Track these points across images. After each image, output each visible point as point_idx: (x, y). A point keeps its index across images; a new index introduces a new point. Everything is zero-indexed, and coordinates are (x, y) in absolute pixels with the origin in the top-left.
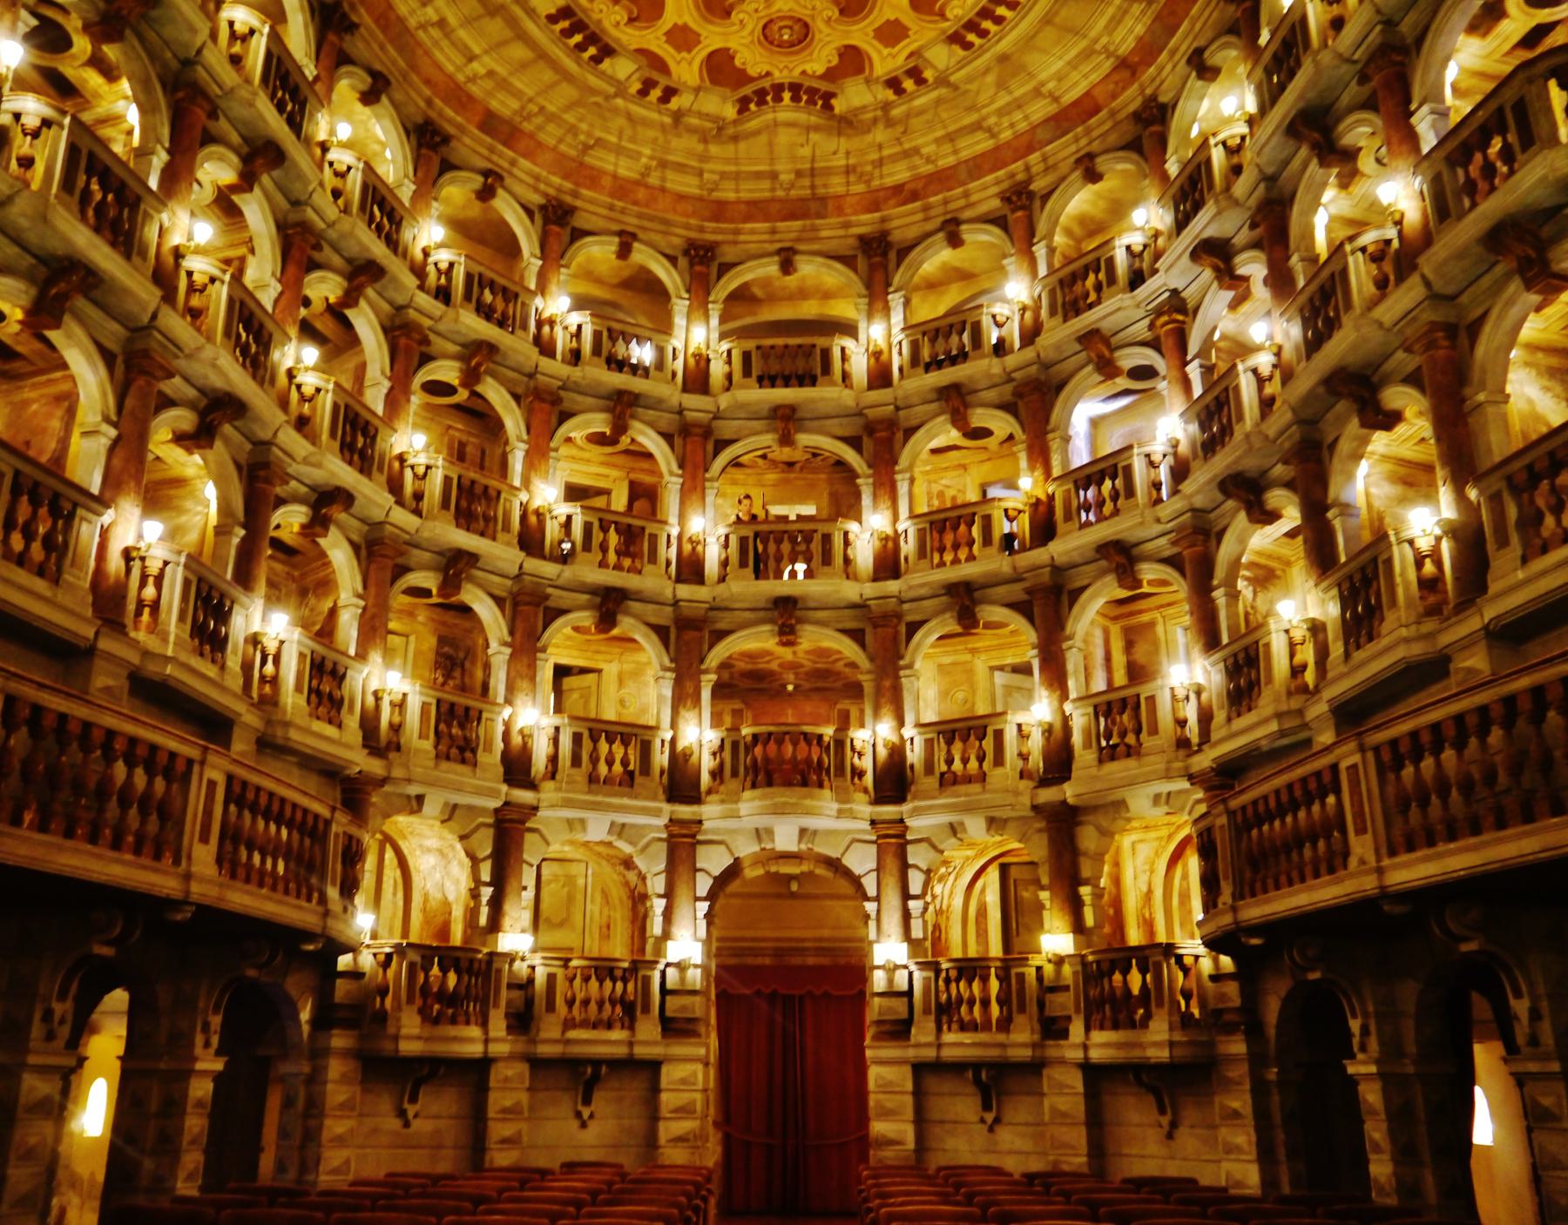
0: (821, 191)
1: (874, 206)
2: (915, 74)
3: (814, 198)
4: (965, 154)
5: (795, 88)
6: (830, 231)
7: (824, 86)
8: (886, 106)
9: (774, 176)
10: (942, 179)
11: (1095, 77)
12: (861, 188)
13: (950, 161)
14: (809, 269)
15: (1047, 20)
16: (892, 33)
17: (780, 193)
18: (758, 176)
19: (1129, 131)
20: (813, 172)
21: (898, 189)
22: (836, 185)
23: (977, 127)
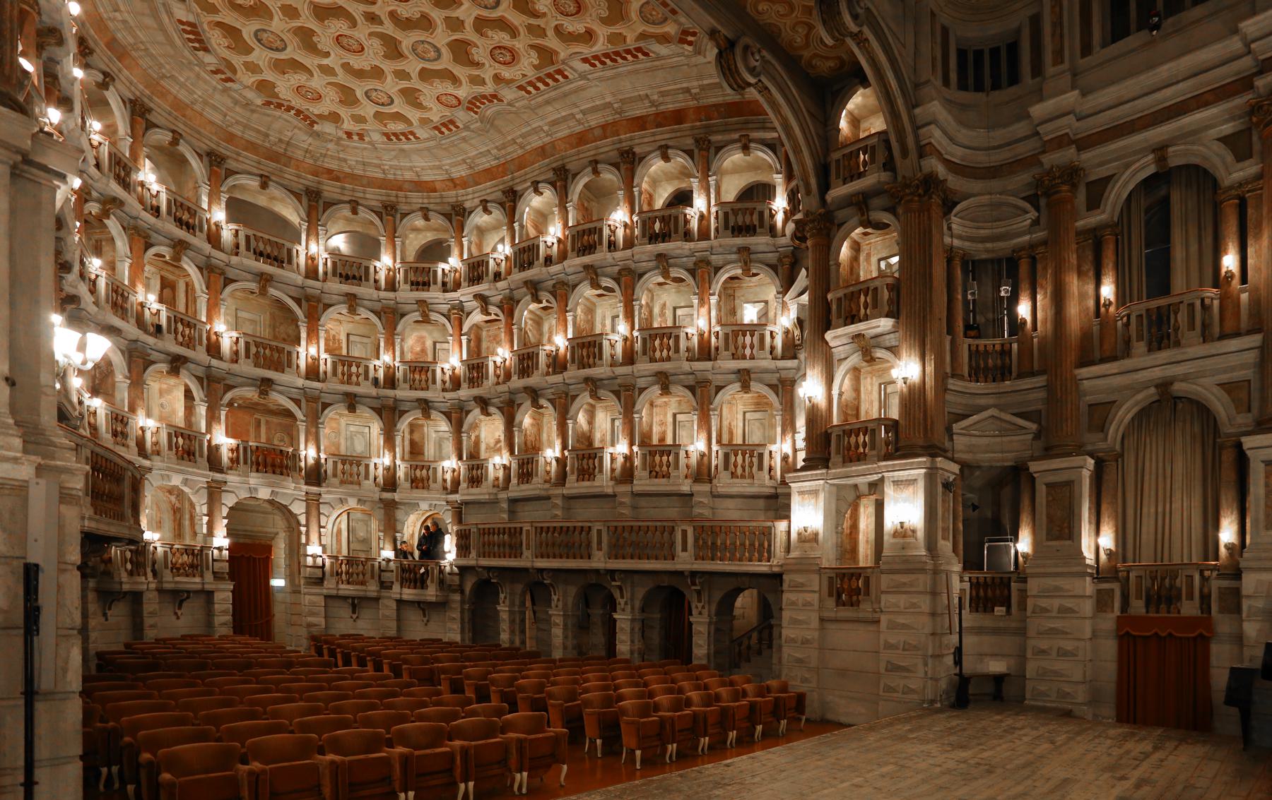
0: (289, 153)
1: (315, 174)
2: (361, 137)
3: (285, 155)
4: (368, 174)
5: (299, 112)
6: (289, 174)
7: (315, 118)
8: (340, 139)
9: (267, 136)
10: (353, 178)
11: (440, 178)
12: (311, 162)
13: (361, 173)
14: (274, 190)
15: (428, 149)
16: (360, 119)
17: (267, 144)
18: (258, 131)
19: (448, 209)
20: (288, 143)
21: (330, 171)
22: (299, 154)
23: (379, 166)
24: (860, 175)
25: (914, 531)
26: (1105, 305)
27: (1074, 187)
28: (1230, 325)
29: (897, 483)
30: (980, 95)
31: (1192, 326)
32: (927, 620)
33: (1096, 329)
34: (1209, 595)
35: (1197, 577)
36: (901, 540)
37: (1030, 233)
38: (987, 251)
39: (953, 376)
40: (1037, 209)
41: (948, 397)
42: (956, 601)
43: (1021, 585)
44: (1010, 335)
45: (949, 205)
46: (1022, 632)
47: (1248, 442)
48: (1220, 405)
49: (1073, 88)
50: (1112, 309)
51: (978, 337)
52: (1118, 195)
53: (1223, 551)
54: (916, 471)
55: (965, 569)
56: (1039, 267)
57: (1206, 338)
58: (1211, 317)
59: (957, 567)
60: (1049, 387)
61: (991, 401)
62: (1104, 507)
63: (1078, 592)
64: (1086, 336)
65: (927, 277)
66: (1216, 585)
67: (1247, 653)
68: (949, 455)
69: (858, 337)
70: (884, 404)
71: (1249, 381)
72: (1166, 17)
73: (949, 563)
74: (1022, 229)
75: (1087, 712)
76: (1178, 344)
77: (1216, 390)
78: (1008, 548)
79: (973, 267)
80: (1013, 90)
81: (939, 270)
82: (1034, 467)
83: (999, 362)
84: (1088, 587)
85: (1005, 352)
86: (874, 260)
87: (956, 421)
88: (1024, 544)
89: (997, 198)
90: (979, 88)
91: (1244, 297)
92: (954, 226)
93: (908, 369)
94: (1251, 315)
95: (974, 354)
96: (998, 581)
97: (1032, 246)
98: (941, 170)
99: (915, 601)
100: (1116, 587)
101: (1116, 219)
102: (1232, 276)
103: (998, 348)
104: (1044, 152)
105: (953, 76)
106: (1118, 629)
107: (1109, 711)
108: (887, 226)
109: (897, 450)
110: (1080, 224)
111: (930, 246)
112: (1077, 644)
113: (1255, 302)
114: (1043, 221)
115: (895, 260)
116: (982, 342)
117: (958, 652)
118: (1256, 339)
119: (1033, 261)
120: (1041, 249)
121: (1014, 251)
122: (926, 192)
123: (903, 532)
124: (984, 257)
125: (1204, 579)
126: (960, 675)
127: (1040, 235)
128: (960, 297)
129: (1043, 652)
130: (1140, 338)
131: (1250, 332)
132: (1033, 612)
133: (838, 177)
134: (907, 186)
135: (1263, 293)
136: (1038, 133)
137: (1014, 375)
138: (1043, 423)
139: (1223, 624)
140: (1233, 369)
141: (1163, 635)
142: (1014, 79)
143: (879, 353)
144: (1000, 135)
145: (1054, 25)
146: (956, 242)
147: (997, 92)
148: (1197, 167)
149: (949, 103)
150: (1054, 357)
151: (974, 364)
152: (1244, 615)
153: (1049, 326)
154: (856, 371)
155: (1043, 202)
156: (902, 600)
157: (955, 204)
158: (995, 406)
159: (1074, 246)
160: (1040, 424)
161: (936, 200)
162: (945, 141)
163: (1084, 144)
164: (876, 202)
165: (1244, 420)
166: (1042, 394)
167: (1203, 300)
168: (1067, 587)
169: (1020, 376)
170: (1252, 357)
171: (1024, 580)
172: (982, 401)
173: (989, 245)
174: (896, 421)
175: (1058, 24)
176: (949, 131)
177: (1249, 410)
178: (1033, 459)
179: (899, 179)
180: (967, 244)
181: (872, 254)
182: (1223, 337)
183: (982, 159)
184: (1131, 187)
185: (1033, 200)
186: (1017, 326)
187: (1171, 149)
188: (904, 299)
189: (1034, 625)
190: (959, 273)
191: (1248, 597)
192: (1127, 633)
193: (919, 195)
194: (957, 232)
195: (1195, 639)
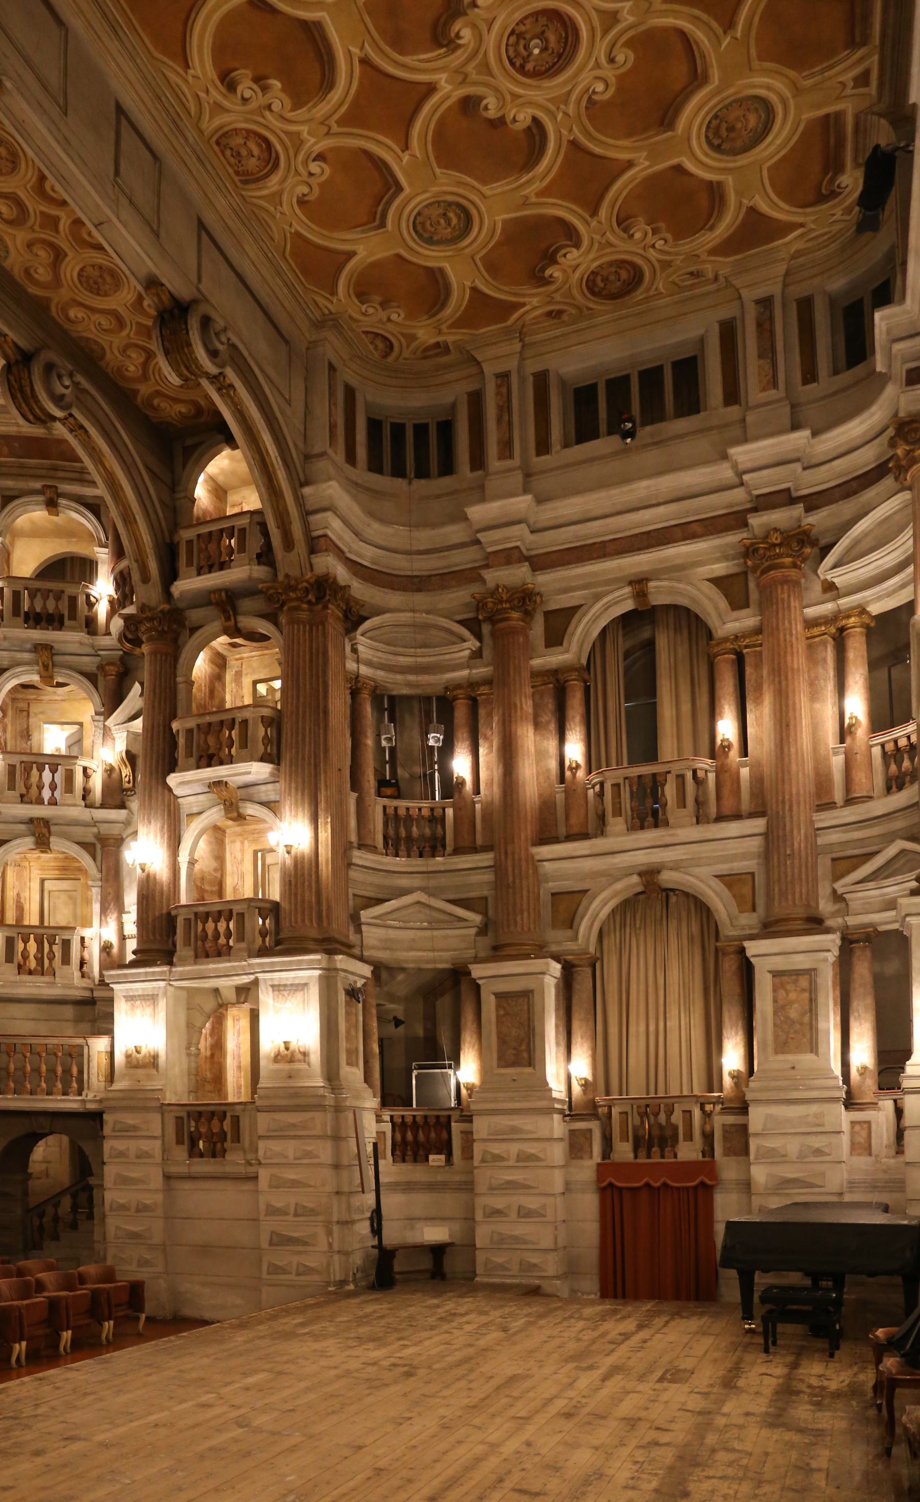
24: (222, 566)
25: (305, 1054)
26: (571, 768)
27: (528, 615)
28: (728, 805)
29: (277, 988)
30: (400, 483)
31: (682, 803)
32: (328, 1173)
33: (560, 798)
34: (712, 1134)
35: (697, 1113)
36: (287, 1067)
37: (469, 667)
38: (409, 685)
39: (361, 846)
40: (479, 637)
41: (353, 874)
42: (370, 1148)
43: (464, 1126)
44: (443, 797)
45: (353, 619)
46: (468, 1186)
47: (753, 948)
48: (720, 901)
49: (526, 491)
50: (581, 774)
51: (398, 796)
52: (587, 633)
53: (727, 1081)
54: (306, 971)
55: (384, 1104)
56: (482, 712)
57: (700, 819)
58: (705, 793)
59: (371, 1102)
60: (497, 868)
61: (416, 881)
62: (576, 1025)
63: (544, 1134)
64: (547, 806)
65: (321, 713)
66: (720, 1121)
67: (756, 1201)
68: (356, 951)
69: (217, 785)
70: (260, 881)
71: (753, 874)
72: (644, 424)
73: (357, 1097)
74: (458, 661)
75: (561, 1288)
76: (666, 824)
77: (715, 883)
78: (446, 1078)
79: (391, 706)
80: (446, 481)
81: (338, 704)
82: (477, 971)
83: (427, 831)
84: (558, 1126)
85: (436, 819)
86: (247, 681)
87: (366, 907)
88: (468, 1071)
89: (423, 617)
90: (399, 472)
91: (745, 772)
92: (360, 648)
93: (293, 833)
94: (753, 795)
95: (392, 819)
96: (432, 1121)
97: (472, 685)
98: (342, 573)
99: (309, 1148)
100: (595, 1126)
101: (584, 661)
102: (729, 746)
103: (426, 813)
104: (487, 566)
105: (361, 452)
106: (600, 1178)
107: (590, 1284)
108: (264, 638)
109: (278, 943)
110: (536, 662)
111: (325, 672)
112: (543, 1198)
113: (758, 780)
114: (487, 653)
115: (277, 684)
116: (403, 804)
117: (377, 1216)
118: (758, 825)
119: (474, 704)
120: (484, 690)
121: (447, 688)
122: (319, 599)
123: (288, 1056)
124: (405, 691)
125: (707, 1115)
126: (380, 1246)
127: (482, 671)
128: (370, 742)
129: (498, 1212)
130: (617, 812)
131: (752, 815)
132: (483, 1161)
133: (190, 563)
134: (294, 589)
135: (766, 771)
136: (478, 542)
137: (449, 849)
138: (491, 913)
139: (728, 1169)
140: (733, 858)
141: (658, 1184)
142: (447, 468)
143: (250, 809)
144: (425, 537)
145: (500, 408)
146: (364, 670)
147: (423, 482)
148: (688, 610)
149: (353, 486)
150: (501, 830)
151: (391, 832)
152: (752, 1157)
153: (496, 790)
154: (218, 834)
155: (486, 629)
156: (290, 1148)
157: (364, 619)
158: (422, 889)
159: (529, 690)
160: (485, 914)
161: (334, 611)
162: (348, 536)
163: (539, 563)
164: (246, 604)
165: (749, 921)
166: (489, 877)
167: (695, 772)
168: (528, 1127)
169: (457, 851)
170: (755, 844)
171: (468, 1119)
172: (404, 882)
173: (411, 678)
174: (276, 906)
175: (505, 408)
176: (352, 522)
177: (754, 909)
178: (477, 960)
179: (281, 577)
180: (380, 674)
181: (244, 674)
182: (720, 818)
183: (401, 565)
184: (603, 623)
185: (473, 626)
186: (451, 787)
187: (652, 584)
188: (288, 737)
189: (484, 1177)
190: (368, 710)
191: (756, 1135)
192: (611, 1184)
193: (309, 602)
194: (365, 655)
195: (695, 1188)
